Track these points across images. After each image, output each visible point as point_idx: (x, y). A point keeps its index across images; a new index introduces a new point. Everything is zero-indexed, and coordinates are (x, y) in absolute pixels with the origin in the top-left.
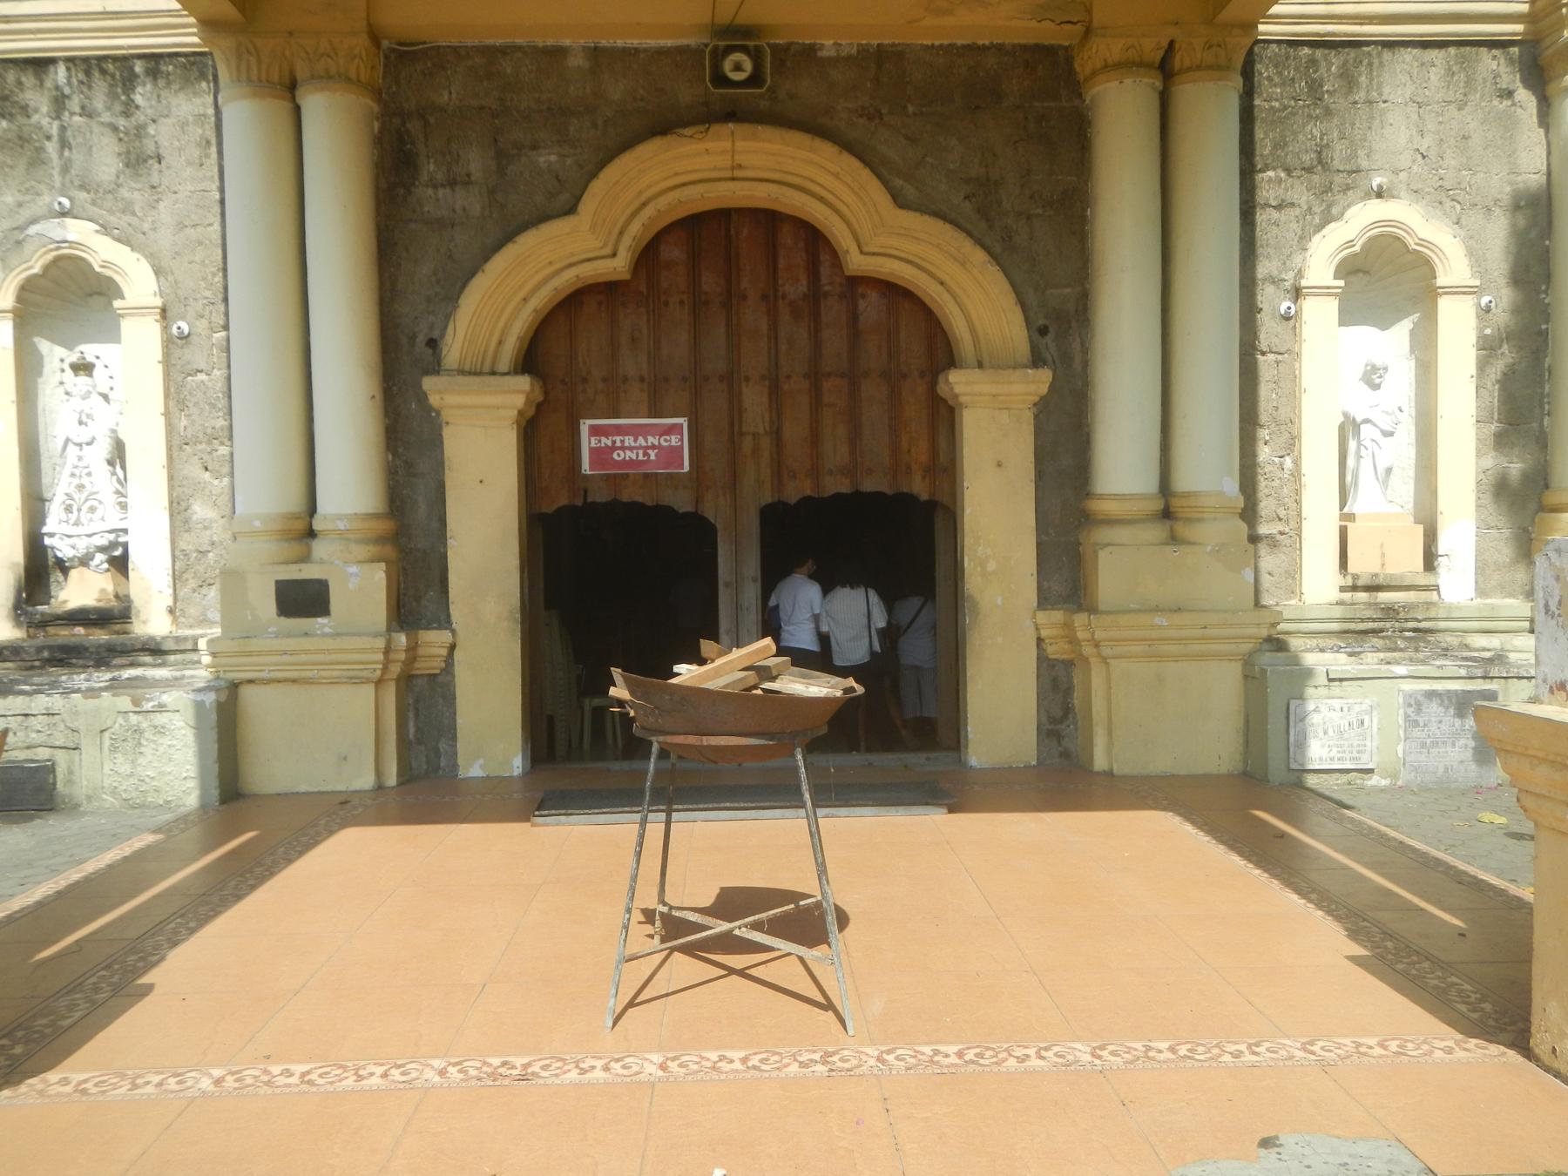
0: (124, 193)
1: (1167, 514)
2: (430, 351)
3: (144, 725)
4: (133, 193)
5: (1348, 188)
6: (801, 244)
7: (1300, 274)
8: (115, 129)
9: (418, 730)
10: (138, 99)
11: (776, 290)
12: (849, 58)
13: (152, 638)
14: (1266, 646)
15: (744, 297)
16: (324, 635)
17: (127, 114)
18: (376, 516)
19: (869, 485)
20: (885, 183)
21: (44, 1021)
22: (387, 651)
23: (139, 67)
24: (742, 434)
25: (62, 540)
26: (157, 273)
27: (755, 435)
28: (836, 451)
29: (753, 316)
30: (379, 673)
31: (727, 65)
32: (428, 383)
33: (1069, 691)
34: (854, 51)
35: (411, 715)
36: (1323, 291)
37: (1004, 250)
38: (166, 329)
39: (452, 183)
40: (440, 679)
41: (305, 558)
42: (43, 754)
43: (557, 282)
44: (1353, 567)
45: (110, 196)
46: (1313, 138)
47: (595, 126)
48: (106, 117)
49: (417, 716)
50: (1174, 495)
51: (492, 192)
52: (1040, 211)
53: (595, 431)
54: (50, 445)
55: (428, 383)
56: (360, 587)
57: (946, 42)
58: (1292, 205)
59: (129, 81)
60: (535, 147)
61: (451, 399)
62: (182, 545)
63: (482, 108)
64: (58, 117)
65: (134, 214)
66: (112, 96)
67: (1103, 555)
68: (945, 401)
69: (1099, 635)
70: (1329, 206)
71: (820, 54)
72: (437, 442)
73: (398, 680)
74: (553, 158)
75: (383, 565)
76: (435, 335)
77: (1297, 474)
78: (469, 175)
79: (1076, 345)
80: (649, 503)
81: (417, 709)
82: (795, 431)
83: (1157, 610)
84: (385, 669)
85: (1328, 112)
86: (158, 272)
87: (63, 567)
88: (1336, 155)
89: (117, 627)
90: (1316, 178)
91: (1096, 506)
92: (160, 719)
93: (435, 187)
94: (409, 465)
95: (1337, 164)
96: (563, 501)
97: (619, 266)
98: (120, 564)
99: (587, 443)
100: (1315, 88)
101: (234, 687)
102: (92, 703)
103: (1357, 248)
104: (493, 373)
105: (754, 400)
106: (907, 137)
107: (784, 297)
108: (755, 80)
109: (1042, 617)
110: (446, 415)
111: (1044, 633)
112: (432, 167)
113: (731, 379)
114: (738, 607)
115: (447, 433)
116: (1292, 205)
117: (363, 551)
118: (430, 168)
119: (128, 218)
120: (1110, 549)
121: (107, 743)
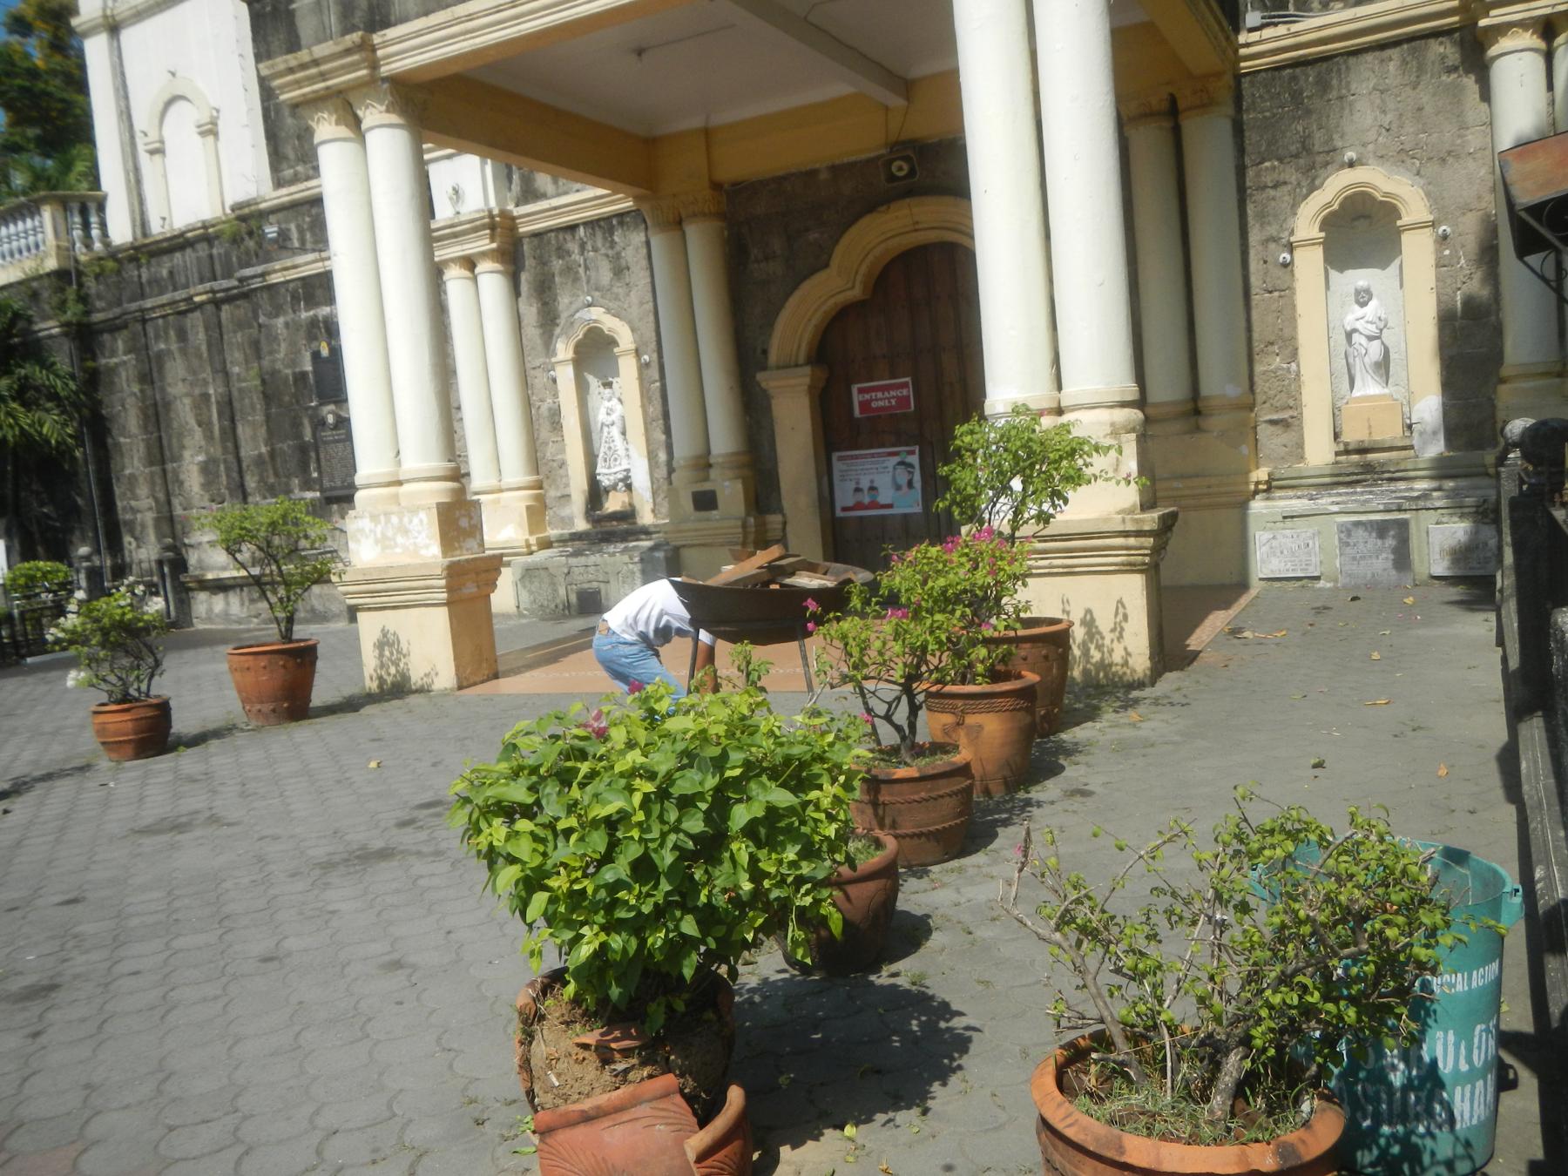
0: (615, 290)
1: (1197, 412)
4: (619, 289)
5: (1327, 164)
7: (1292, 233)
10: (616, 239)
17: (612, 247)
22: (744, 526)
23: (615, 222)
25: (606, 476)
31: (894, 169)
32: (760, 376)
36: (1310, 243)
39: (767, 259)
41: (707, 479)
42: (595, 585)
43: (825, 308)
44: (1345, 438)
48: (603, 251)
53: (861, 391)
54: (595, 428)
55: (760, 376)
56: (731, 493)
59: (611, 231)
66: (605, 239)
70: (1313, 180)
72: (769, 409)
85: (1309, 112)
86: (633, 330)
87: (607, 492)
88: (1317, 143)
90: (1302, 161)
95: (1317, 148)
97: (856, 293)
98: (629, 487)
99: (856, 398)
100: (1297, 97)
101: (677, 549)
103: (1336, 207)
104: (797, 366)
108: (912, 173)
115: (774, 402)
116: (1285, 183)
118: (755, 252)
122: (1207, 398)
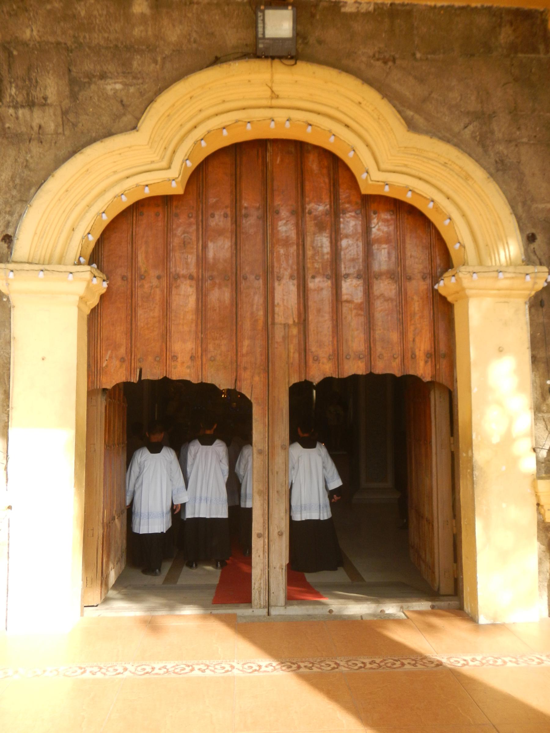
6: (325, 171)
11: (303, 209)
12: (367, 14)
19: (380, 368)
27: (286, 326)
29: (285, 228)
34: (371, 8)
39: (31, 104)
47: (156, 62)
51: (65, 113)
57: (446, 4)
60: (103, 76)
63: (58, 43)
71: (343, 10)
76: (10, 232)
78: (45, 98)
93: (15, 107)
106: (415, 78)
107: (310, 213)
110: (15, 300)
112: (13, 91)
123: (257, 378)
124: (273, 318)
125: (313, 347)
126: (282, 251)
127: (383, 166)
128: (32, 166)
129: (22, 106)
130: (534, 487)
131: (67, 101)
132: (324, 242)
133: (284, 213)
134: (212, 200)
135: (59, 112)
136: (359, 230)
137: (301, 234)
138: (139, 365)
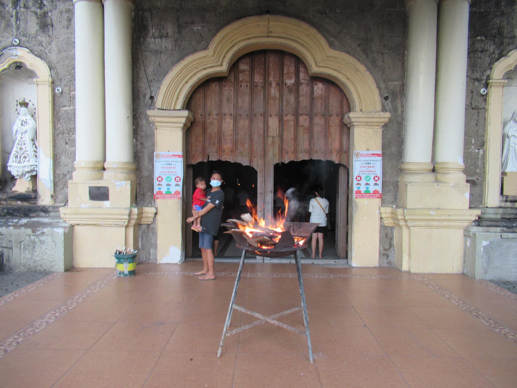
0: (39, 38)
2: (151, 101)
3: (37, 240)
4: (42, 38)
6: (293, 64)
8: (36, 14)
9: (142, 244)
13: (44, 207)
14: (474, 224)
15: (271, 84)
16: (106, 208)
17: (40, 8)
18: (128, 163)
20: (327, 39)
21: (31, 329)
22: (130, 215)
24: (268, 136)
26: (50, 69)
27: (273, 137)
28: (304, 142)
29: (274, 91)
30: (126, 223)
33: (391, 239)
35: (140, 239)
37: (373, 66)
38: (53, 90)
39: (161, 37)
40: (151, 226)
41: (101, 178)
45: (34, 39)
46: (497, 24)
47: (216, 15)
48: (33, 9)
49: (142, 240)
50: (436, 163)
51: (176, 41)
52: (387, 51)
55: (150, 112)
56: (121, 189)
58: (487, 51)
60: (192, 23)
61: (157, 119)
62: (57, 172)
63: (173, 8)
64: (15, 8)
65: (42, 46)
67: (409, 187)
68: (346, 125)
69: (407, 218)
72: (152, 135)
73: (135, 226)
74: (200, 28)
75: (129, 182)
76: (153, 95)
77: (484, 157)
78: (167, 34)
79: (399, 104)
80: (232, 162)
81: (142, 237)
82: (289, 135)
83: (431, 209)
84: (129, 222)
88: (505, 31)
89: (33, 202)
91: (405, 166)
92: (43, 238)
93: (155, 38)
94: (142, 144)
96: (200, 160)
98: (34, 178)
101: (72, 226)
102: (17, 231)
105: (273, 123)
107: (286, 84)
109: (383, 209)
111: (383, 216)
112: (154, 30)
113: (265, 116)
114: (264, 202)
116: (487, 51)
117: (122, 176)
118: (153, 31)
119: (41, 48)
120: (412, 184)
121: (22, 247)
122: (443, 163)
123: (260, 161)
124: (267, 134)
125: (285, 147)
126: (272, 103)
127: (319, 64)
128: (162, 64)
129: (157, 38)
130: (380, 209)
131: (177, 35)
132: (292, 98)
133: (274, 84)
134: (241, 79)
135: (173, 40)
136: (308, 93)
137: (281, 96)
138: (207, 154)
